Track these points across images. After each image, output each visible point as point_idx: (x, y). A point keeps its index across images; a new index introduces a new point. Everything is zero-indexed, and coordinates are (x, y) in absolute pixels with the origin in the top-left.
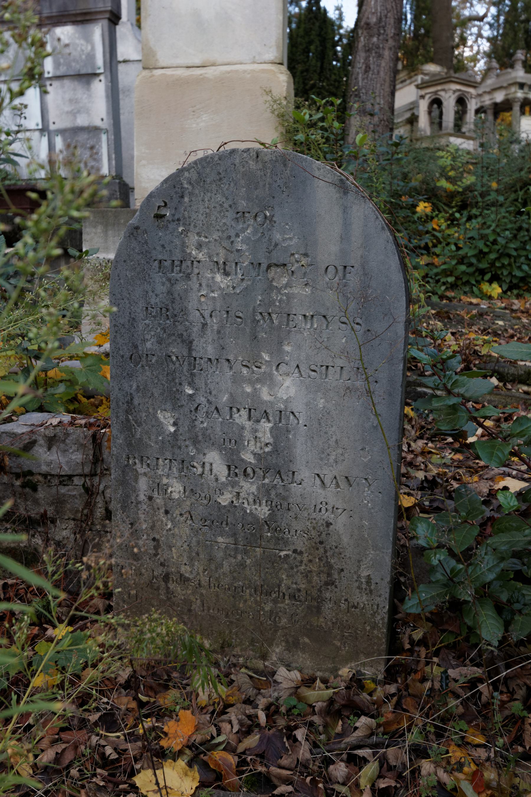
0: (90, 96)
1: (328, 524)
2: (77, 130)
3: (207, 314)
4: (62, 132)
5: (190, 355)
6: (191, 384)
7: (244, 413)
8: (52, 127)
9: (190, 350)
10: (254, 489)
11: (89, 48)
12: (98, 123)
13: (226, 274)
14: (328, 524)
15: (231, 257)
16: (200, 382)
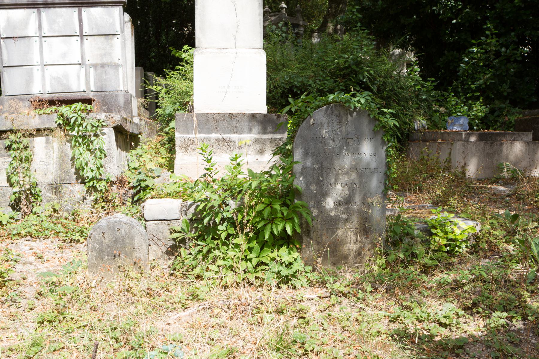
0: (111, 46)
1: (366, 218)
2: (102, 66)
3: (327, 154)
4: (95, 66)
5: (322, 167)
6: (322, 177)
7: (339, 185)
8: (87, 63)
9: (322, 165)
10: (342, 209)
11: (111, 20)
12: (117, 61)
13: (334, 141)
14: (366, 218)
15: (336, 136)
16: (325, 175)
